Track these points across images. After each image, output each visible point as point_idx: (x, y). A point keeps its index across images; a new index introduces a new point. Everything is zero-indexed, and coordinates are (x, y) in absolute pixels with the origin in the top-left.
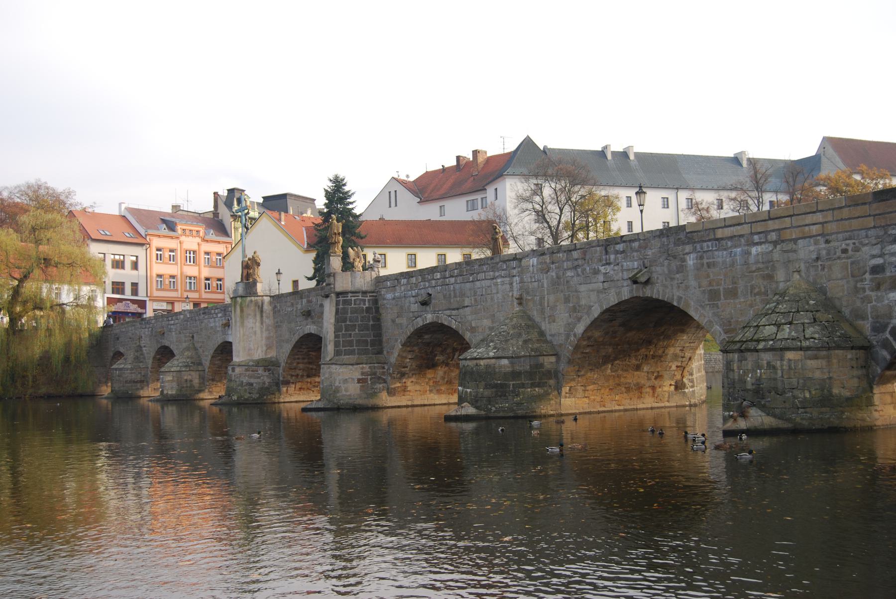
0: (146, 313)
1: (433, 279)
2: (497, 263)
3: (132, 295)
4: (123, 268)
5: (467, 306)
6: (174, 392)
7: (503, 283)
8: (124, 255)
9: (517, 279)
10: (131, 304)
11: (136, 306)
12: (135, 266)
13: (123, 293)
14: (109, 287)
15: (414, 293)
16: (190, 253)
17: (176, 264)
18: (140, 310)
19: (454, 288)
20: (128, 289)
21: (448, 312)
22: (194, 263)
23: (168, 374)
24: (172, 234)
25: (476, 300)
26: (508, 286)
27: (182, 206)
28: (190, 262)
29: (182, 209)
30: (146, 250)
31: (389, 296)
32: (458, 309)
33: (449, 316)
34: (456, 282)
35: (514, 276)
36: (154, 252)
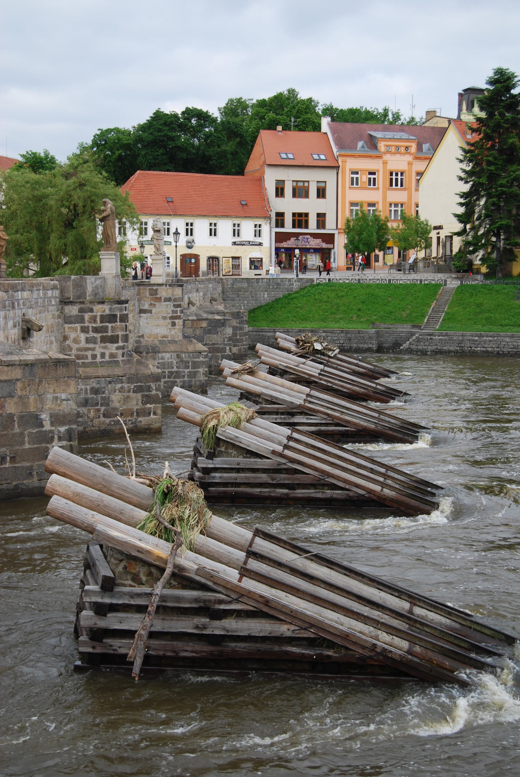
0: (334, 248)
3: (318, 228)
4: (307, 196)
8: (308, 182)
10: (311, 239)
11: (319, 241)
12: (321, 193)
13: (307, 227)
14: (288, 220)
16: (397, 174)
17: (378, 189)
18: (324, 245)
20: (313, 221)
22: (402, 185)
24: (374, 153)
27: (438, 111)
28: (397, 185)
29: (438, 114)
30: (338, 173)
36: (348, 176)
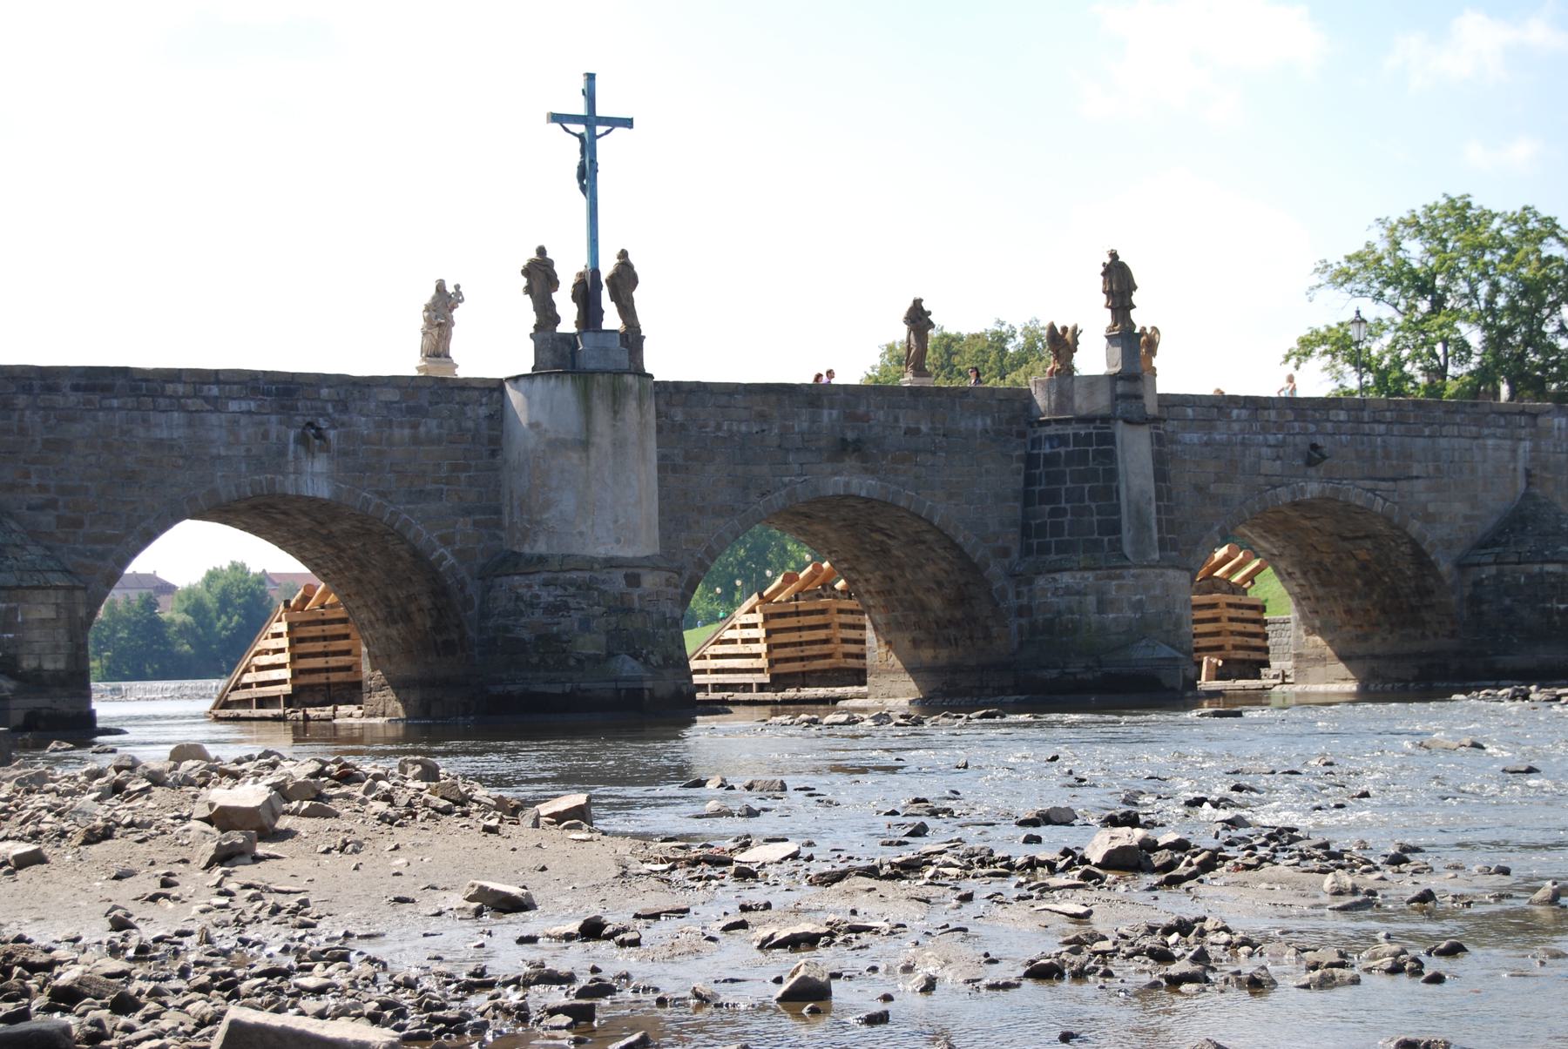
1: (1328, 420)
2: (1487, 414)
5: (1417, 477)
6: (61, 665)
7: (1497, 448)
9: (1527, 444)
15: (1271, 439)
19: (1384, 441)
21: (1369, 484)
23: (39, 595)
25: (1437, 469)
26: (1507, 455)
31: (1192, 437)
32: (1394, 480)
33: (1372, 491)
34: (1389, 433)
35: (1521, 439)
